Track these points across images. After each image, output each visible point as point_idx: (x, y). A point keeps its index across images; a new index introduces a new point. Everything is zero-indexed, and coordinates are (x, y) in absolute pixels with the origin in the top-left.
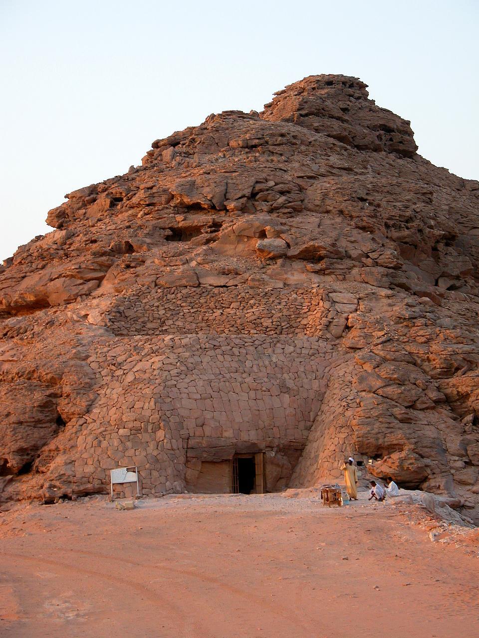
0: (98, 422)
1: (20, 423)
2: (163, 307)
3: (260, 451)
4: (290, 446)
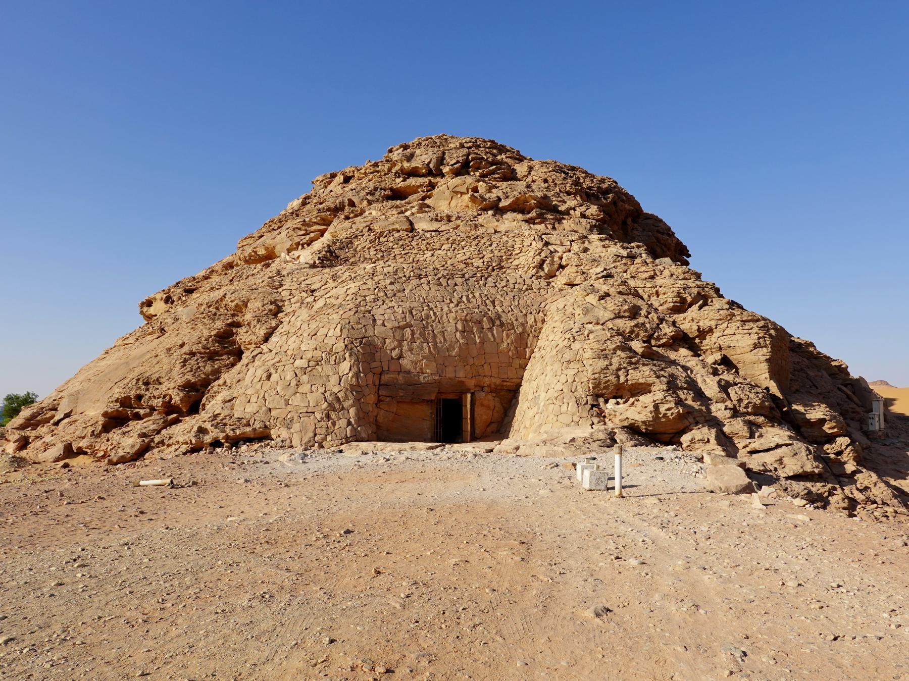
0: (274, 352)
1: (193, 354)
2: (375, 249)
3: (468, 391)
4: (503, 386)
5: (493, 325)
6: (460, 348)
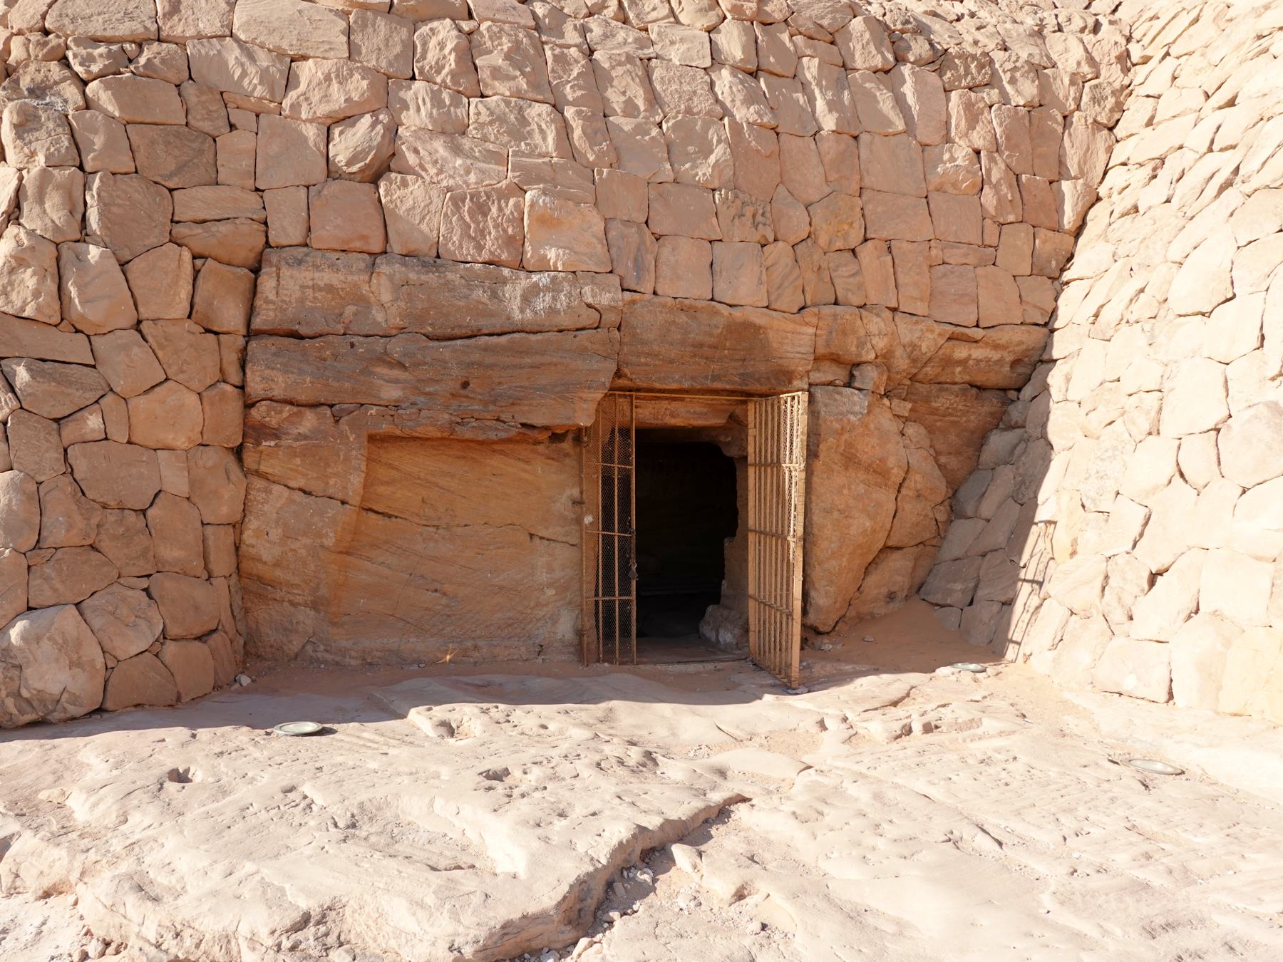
4: (948, 362)
5: (900, 59)
6: (736, 141)
